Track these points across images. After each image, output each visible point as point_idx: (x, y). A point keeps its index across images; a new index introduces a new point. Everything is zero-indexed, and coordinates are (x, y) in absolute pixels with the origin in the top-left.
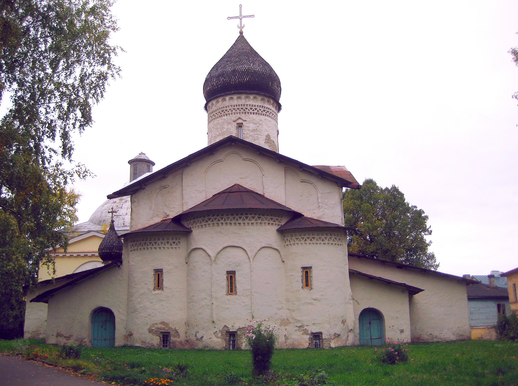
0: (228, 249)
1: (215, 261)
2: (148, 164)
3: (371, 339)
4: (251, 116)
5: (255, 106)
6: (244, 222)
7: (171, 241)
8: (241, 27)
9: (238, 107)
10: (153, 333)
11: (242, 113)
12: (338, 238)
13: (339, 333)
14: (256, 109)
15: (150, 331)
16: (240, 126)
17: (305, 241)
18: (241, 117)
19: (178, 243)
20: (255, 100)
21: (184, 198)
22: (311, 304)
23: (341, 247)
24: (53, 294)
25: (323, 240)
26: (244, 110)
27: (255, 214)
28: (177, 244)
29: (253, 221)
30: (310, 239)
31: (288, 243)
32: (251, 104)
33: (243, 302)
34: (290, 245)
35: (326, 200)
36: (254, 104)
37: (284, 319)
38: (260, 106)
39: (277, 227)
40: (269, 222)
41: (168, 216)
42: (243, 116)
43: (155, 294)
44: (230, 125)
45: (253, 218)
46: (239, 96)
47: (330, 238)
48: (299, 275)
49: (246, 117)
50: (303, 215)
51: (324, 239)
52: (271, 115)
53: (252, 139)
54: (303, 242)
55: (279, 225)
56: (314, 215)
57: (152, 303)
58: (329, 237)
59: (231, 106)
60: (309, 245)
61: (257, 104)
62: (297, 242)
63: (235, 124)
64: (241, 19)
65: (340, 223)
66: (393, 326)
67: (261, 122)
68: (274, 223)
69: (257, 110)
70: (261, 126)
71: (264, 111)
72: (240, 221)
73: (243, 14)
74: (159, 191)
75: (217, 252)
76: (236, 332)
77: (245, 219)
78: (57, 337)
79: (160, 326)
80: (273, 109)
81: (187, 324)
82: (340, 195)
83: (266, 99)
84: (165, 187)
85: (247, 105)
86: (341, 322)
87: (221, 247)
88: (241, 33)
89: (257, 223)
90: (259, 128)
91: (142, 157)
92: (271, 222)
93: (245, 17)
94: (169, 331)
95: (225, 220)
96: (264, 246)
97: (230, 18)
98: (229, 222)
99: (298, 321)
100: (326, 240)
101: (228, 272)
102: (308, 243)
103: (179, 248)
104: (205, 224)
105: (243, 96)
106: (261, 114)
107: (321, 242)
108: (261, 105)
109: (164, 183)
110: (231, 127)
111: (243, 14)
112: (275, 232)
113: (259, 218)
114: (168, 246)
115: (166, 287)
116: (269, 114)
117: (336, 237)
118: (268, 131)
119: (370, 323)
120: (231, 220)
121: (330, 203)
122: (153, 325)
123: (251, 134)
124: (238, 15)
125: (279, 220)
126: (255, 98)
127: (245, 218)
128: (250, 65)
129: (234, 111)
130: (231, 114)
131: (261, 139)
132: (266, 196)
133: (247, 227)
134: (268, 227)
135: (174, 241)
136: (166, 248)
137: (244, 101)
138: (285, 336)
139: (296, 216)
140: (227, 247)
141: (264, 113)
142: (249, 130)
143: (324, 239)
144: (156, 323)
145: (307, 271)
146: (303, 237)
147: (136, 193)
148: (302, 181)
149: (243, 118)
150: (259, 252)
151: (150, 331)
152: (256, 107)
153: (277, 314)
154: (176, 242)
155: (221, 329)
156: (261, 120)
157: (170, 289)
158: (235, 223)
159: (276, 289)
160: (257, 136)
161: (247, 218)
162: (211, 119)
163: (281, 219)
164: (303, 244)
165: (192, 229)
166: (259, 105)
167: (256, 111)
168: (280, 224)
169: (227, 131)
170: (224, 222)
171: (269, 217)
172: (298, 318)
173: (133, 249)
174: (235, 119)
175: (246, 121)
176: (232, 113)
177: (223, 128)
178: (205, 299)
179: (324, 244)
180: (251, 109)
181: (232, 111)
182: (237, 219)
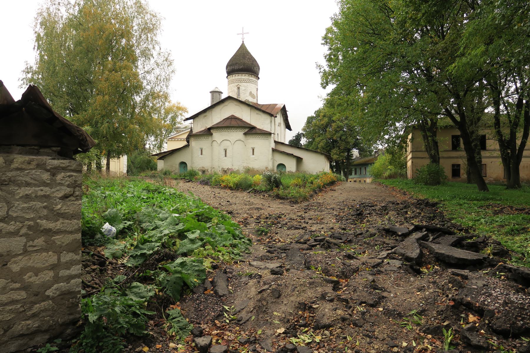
8: (243, 39)
16: (239, 88)
42: (240, 84)
73: (244, 32)
80: (255, 79)
83: (250, 75)
88: (243, 42)
91: (217, 90)
97: (238, 34)
105: (240, 75)
109: (205, 114)
111: (244, 32)
124: (242, 33)
132: (243, 120)
134: (240, 133)
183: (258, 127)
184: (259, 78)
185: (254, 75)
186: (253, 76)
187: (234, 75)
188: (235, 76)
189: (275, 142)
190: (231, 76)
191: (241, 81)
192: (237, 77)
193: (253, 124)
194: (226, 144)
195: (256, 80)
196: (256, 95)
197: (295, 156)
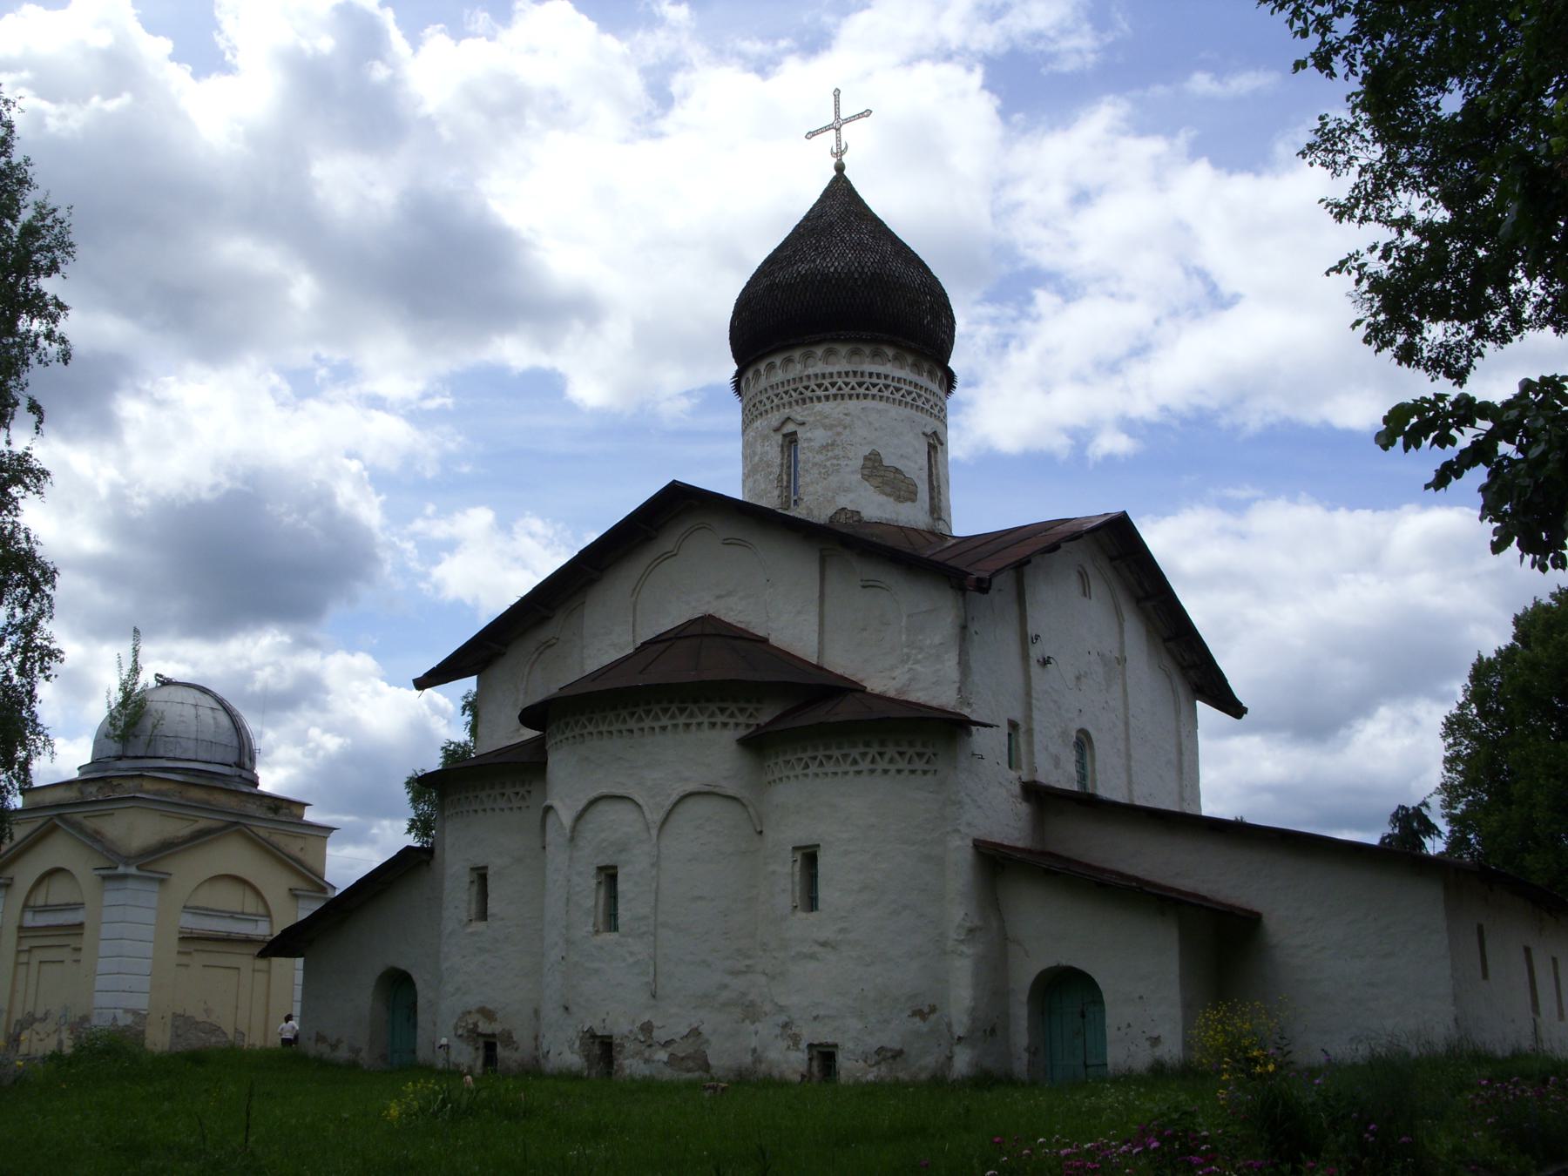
0: (602, 807)
1: (572, 839)
3: (1086, 1066)
4: (818, 406)
5: (831, 375)
6: (641, 725)
7: (509, 791)
8: (839, 153)
9: (786, 388)
11: (797, 402)
12: (910, 752)
13: (897, 1047)
17: (804, 769)
18: (793, 415)
19: (526, 794)
20: (832, 359)
22: (812, 957)
25: (855, 762)
27: (671, 702)
28: (523, 798)
29: (665, 721)
30: (818, 761)
33: (632, 954)
35: (920, 637)
36: (828, 369)
38: (847, 374)
39: (742, 732)
40: (713, 720)
42: (798, 413)
43: (472, 934)
44: (767, 444)
45: (665, 711)
46: (786, 355)
48: (787, 870)
49: (806, 413)
50: (863, 690)
51: (858, 757)
53: (820, 473)
55: (748, 726)
56: (894, 682)
58: (873, 750)
60: (913, 776)
61: (835, 369)
63: (779, 438)
65: (953, 703)
68: (732, 721)
70: (848, 430)
72: (632, 724)
74: (535, 655)
77: (644, 716)
78: (316, 1044)
83: (867, 350)
84: (548, 644)
85: (809, 377)
86: (909, 1012)
87: (584, 802)
88: (840, 168)
89: (675, 726)
90: (843, 437)
92: (720, 719)
96: (691, 787)
97: (811, 135)
98: (604, 728)
99: (781, 1009)
100: (845, 762)
101: (600, 869)
103: (528, 807)
105: (797, 354)
107: (846, 767)
108: (849, 368)
109: (545, 634)
110: (769, 448)
111: (843, 116)
112: (734, 746)
113: (682, 711)
116: (880, 390)
117: (901, 749)
119: (1083, 1016)
120: (611, 724)
121: (928, 642)
123: (819, 458)
124: (830, 119)
127: (676, 711)
128: (814, 261)
131: (848, 469)
132: (775, 640)
134: (707, 734)
135: (516, 790)
136: (497, 810)
138: (754, 1050)
139: (839, 689)
141: (862, 391)
144: (468, 1009)
145: (809, 858)
146: (799, 755)
148: (861, 584)
153: (725, 986)
154: (522, 791)
156: (846, 414)
157: (502, 919)
158: (620, 731)
159: (726, 916)
160: (835, 462)
161: (648, 712)
164: (800, 777)
167: (833, 391)
168: (752, 721)
169: (761, 460)
170: (595, 731)
171: (713, 707)
172: (782, 1001)
174: (775, 423)
175: (803, 424)
176: (772, 408)
178: (556, 944)
179: (859, 772)
180: (819, 386)
181: (773, 401)
182: (625, 718)
183: (875, 685)
185: (892, 343)
186: (890, 352)
188: (771, 367)
192: (779, 376)
193: (842, 661)
194: (615, 823)
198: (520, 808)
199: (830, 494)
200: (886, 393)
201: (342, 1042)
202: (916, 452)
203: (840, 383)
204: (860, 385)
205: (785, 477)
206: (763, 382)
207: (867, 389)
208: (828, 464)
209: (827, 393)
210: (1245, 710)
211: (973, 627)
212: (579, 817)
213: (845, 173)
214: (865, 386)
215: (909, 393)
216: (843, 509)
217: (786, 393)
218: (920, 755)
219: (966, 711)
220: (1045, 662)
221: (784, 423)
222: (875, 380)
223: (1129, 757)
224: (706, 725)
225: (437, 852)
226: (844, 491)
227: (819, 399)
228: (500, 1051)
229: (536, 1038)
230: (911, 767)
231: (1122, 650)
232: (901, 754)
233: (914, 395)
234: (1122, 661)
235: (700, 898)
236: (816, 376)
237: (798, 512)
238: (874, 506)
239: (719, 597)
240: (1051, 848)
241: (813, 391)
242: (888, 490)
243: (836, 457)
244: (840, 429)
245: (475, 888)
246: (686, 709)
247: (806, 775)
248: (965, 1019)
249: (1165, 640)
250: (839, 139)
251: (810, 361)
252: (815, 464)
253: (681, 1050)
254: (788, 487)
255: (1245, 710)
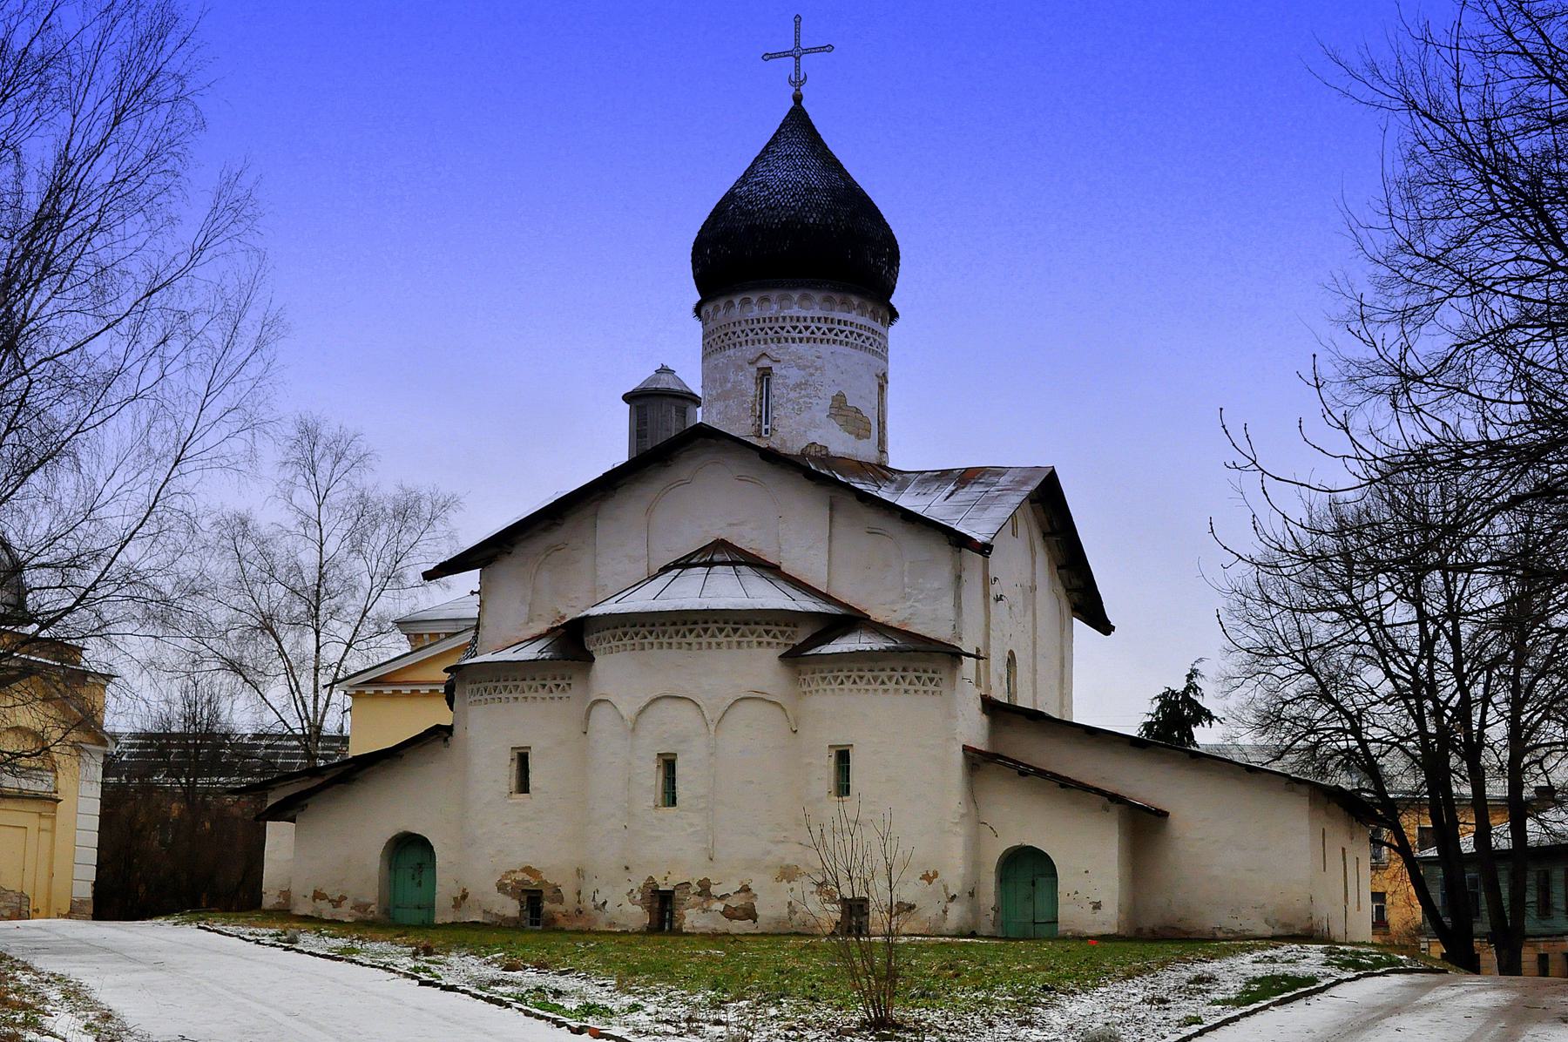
0: (663, 705)
1: (633, 729)
2: (679, 402)
4: (794, 347)
7: (550, 683)
8: (798, 82)
9: (762, 325)
10: (506, 893)
11: (772, 340)
14: (807, 328)
15: (501, 887)
20: (806, 303)
21: (599, 573)
23: (937, 697)
24: (306, 802)
25: (883, 683)
26: (776, 332)
28: (564, 689)
29: (721, 638)
30: (851, 680)
31: (805, 688)
32: (795, 315)
33: (691, 825)
34: (811, 692)
35: (921, 580)
36: (803, 313)
37: (788, 866)
38: (819, 319)
39: (783, 651)
41: (563, 617)
42: (772, 349)
46: (765, 294)
47: (902, 677)
51: (886, 680)
52: (851, 340)
54: (835, 686)
57: (506, 824)
59: (747, 321)
61: (809, 314)
62: (823, 686)
64: (797, 59)
66: (1076, 893)
67: (819, 363)
69: (810, 330)
71: (830, 330)
74: (544, 557)
75: (636, 708)
76: (673, 892)
78: (314, 900)
79: (520, 876)
81: (580, 873)
82: (954, 567)
83: (837, 297)
85: (784, 318)
87: (647, 699)
88: (798, 99)
91: (665, 383)
92: (766, 639)
93: (808, 51)
94: (539, 888)
95: (658, 637)
98: (665, 640)
102: (846, 691)
104: (617, 643)
105: (774, 295)
106: (821, 341)
108: (821, 314)
112: (776, 661)
114: (543, 693)
115: (536, 788)
116: (846, 337)
118: (838, 385)
119: (1033, 885)
120: (671, 637)
121: (929, 586)
122: (506, 876)
123: (793, 395)
125: (789, 632)
126: (804, 297)
129: (750, 335)
130: (744, 343)
131: (818, 407)
133: (705, 652)
137: (775, 307)
140: (658, 698)
141: (831, 336)
142: (786, 386)
143: (886, 680)
145: (843, 757)
147: (491, 563)
149: (773, 354)
150: (730, 711)
151: (501, 887)
152: (809, 323)
153: (769, 853)
154: (563, 683)
155: (641, 885)
160: (809, 400)
162: (709, 350)
163: (793, 632)
165: (595, 656)
166: (816, 316)
167: (807, 334)
169: (734, 387)
173: (473, 699)
176: (747, 341)
177: (726, 380)
178: (613, 815)
179: (886, 691)
180: (794, 328)
181: (747, 335)
184: (894, 315)
186: (855, 301)
187: (737, 300)
188: (747, 301)
189: (990, 706)
190: (722, 303)
191: (778, 332)
192: (755, 312)
195: (877, 326)
196: (870, 412)
197: (1115, 798)
198: (561, 698)
199: (802, 429)
200: (851, 340)
201: (346, 898)
202: (871, 393)
203: (813, 327)
204: (830, 330)
205: (758, 407)
206: (736, 313)
207: (836, 335)
208: (801, 401)
209: (801, 335)
210: (1113, 628)
211: (965, 576)
212: (642, 712)
213: (803, 103)
214: (835, 332)
215: (868, 338)
216: (814, 443)
217: (762, 330)
218: (931, 680)
219: (958, 644)
220: (999, 599)
221: (758, 359)
222: (842, 327)
223: (1035, 671)
224: (755, 644)
225: (456, 731)
226: (815, 427)
227: (794, 340)
228: (547, 906)
229: (579, 893)
230: (925, 688)
231: (1033, 581)
232: (918, 678)
233: (872, 340)
234: (1033, 589)
235: (752, 782)
236: (791, 318)
237: (774, 443)
238: (840, 443)
239: (730, 525)
240: (1000, 751)
241: (788, 332)
242: (850, 428)
243: (809, 396)
244: (812, 371)
245: (515, 765)
246: (738, 629)
247: (843, 689)
248: (959, 884)
249: (1059, 568)
250: (797, 68)
251: (785, 303)
252: (789, 400)
253: (734, 902)
254: (760, 417)
255: (1113, 628)
